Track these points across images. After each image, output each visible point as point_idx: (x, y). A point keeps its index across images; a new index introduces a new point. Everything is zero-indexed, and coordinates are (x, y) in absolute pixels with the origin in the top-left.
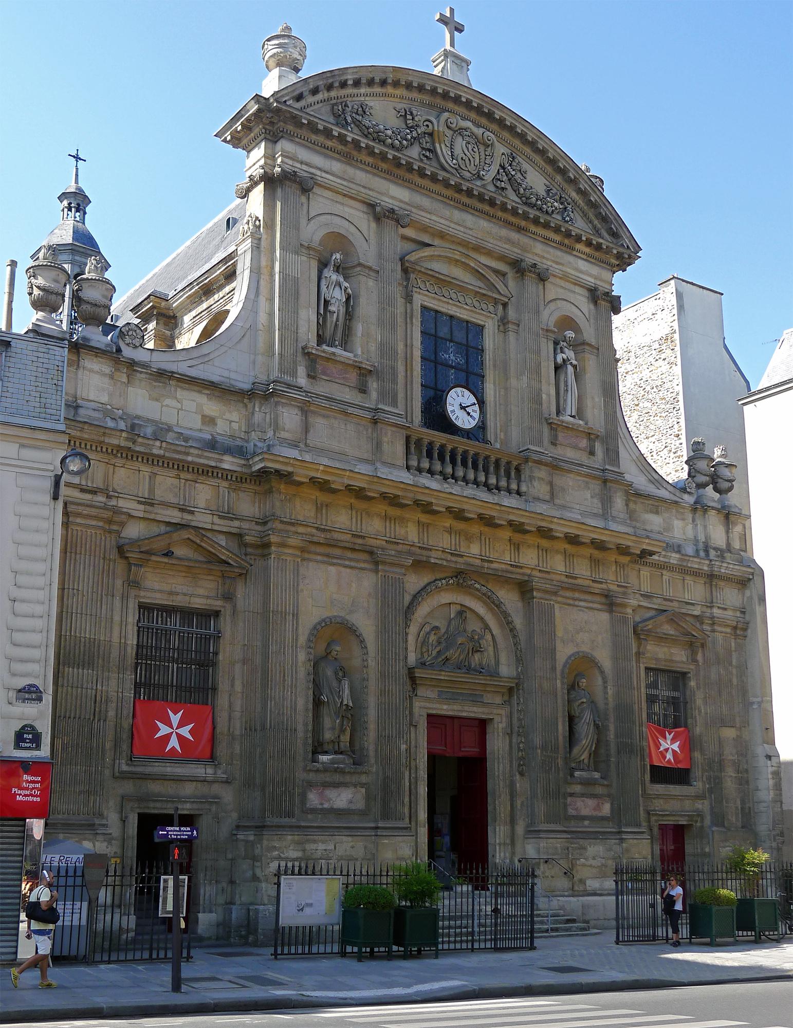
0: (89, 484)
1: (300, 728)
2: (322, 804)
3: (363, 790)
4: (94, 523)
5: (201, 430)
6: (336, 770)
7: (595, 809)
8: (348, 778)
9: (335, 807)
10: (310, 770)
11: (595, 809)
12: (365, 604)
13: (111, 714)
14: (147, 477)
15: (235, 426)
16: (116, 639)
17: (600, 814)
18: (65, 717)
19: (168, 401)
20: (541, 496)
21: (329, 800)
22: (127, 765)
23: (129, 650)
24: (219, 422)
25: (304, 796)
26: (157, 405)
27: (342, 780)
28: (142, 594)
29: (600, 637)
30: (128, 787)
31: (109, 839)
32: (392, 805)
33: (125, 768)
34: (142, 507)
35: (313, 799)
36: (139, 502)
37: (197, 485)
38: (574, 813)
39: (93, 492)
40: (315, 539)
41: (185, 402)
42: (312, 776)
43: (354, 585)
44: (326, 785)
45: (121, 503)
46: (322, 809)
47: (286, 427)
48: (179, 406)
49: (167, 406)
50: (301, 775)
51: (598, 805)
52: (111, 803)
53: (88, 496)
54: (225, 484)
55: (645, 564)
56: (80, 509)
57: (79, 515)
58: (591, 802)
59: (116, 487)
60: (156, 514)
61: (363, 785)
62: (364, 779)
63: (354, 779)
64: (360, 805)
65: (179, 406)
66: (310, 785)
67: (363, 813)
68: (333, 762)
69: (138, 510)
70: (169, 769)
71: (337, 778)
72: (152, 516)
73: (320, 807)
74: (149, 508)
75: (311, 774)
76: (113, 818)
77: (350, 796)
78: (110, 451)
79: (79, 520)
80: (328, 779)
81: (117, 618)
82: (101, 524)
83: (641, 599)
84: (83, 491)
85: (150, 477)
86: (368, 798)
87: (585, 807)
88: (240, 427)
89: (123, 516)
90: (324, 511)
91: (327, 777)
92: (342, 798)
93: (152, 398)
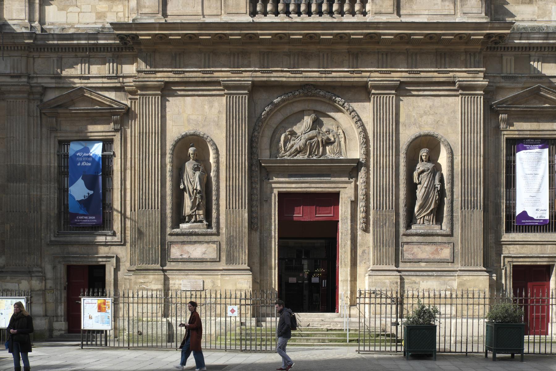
0: (16, 72)
4: (21, 95)
5: (95, 23)
7: (432, 253)
11: (432, 253)
12: (216, 119)
13: (43, 208)
14: (56, 61)
15: (121, 15)
16: (44, 164)
17: (439, 257)
18: (10, 211)
19: (71, 9)
20: (383, 11)
22: (54, 236)
23: (52, 170)
24: (109, 15)
26: (64, 13)
28: (59, 135)
29: (446, 117)
30: (56, 250)
31: (43, 278)
32: (236, 254)
33: (53, 239)
34: (53, 81)
36: (52, 78)
37: (91, 59)
38: (410, 257)
39: (19, 76)
40: (171, 80)
41: (83, 7)
43: (206, 107)
45: (40, 80)
47: (147, 4)
48: (79, 10)
49: (71, 12)
51: (437, 249)
52: (46, 259)
53: (16, 80)
54: (110, 54)
55: (506, 49)
56: (8, 88)
57: (10, 92)
58: (428, 248)
59: (36, 71)
60: (63, 83)
65: (79, 10)
67: (213, 261)
68: (190, 228)
69: (51, 83)
70: (81, 238)
72: (61, 85)
73: (181, 257)
74: (58, 80)
76: (48, 268)
77: (204, 250)
78: (23, 48)
79: (11, 95)
81: (44, 151)
82: (26, 95)
83: (502, 80)
84: (12, 77)
85: (57, 60)
87: (424, 252)
88: (124, 15)
89: (39, 88)
90: (178, 59)
92: (197, 251)
93: (60, 9)
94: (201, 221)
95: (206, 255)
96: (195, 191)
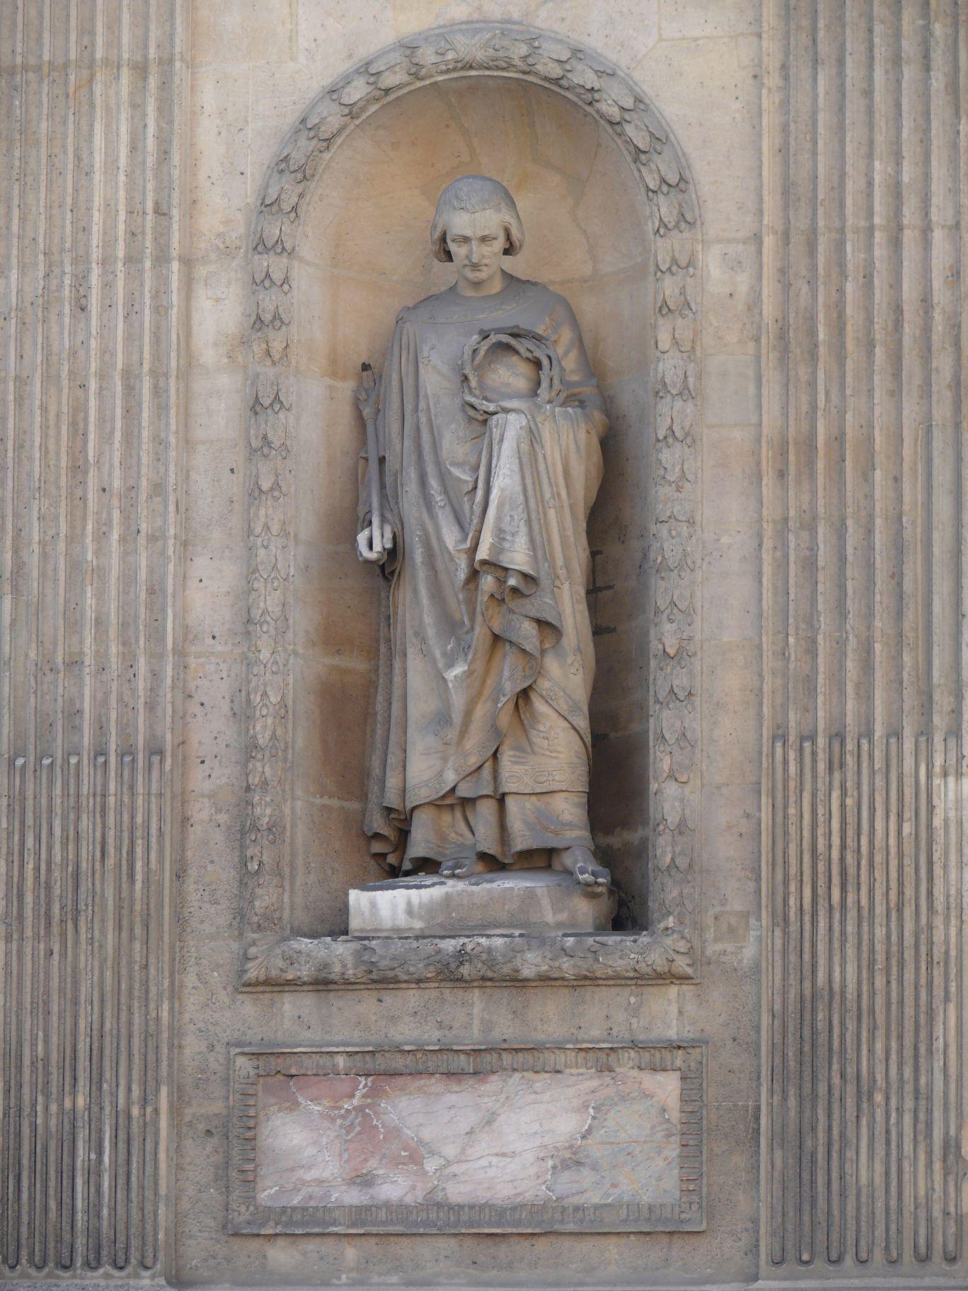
1: (211, 732)
2: (365, 1181)
3: (667, 1087)
6: (450, 975)
8: (549, 1017)
9: (457, 1193)
10: (275, 985)
21: (414, 1156)
25: (238, 1140)
27: (506, 1029)
35: (305, 1149)
42: (294, 1018)
44: (385, 1067)
46: (360, 1214)
50: (209, 1015)
61: (655, 1054)
62: (668, 1013)
63: (602, 1015)
64: (646, 1174)
66: (279, 1070)
68: (447, 923)
71: (475, 1018)
73: (354, 1197)
75: (291, 1006)
77: (566, 1125)
80: (406, 1032)
86: (694, 1132)
91: (407, 1019)
94: (541, 859)
95: (587, 1177)
96: (488, 582)
